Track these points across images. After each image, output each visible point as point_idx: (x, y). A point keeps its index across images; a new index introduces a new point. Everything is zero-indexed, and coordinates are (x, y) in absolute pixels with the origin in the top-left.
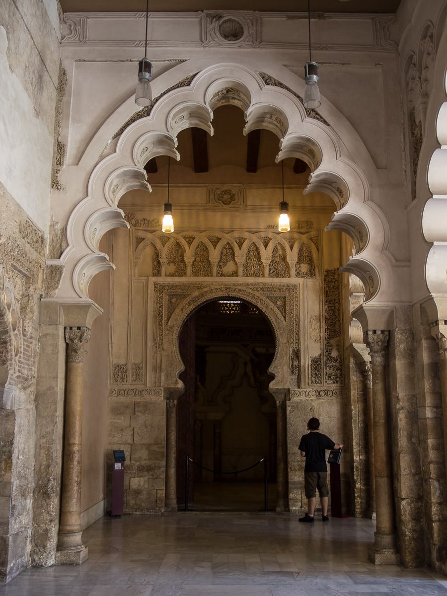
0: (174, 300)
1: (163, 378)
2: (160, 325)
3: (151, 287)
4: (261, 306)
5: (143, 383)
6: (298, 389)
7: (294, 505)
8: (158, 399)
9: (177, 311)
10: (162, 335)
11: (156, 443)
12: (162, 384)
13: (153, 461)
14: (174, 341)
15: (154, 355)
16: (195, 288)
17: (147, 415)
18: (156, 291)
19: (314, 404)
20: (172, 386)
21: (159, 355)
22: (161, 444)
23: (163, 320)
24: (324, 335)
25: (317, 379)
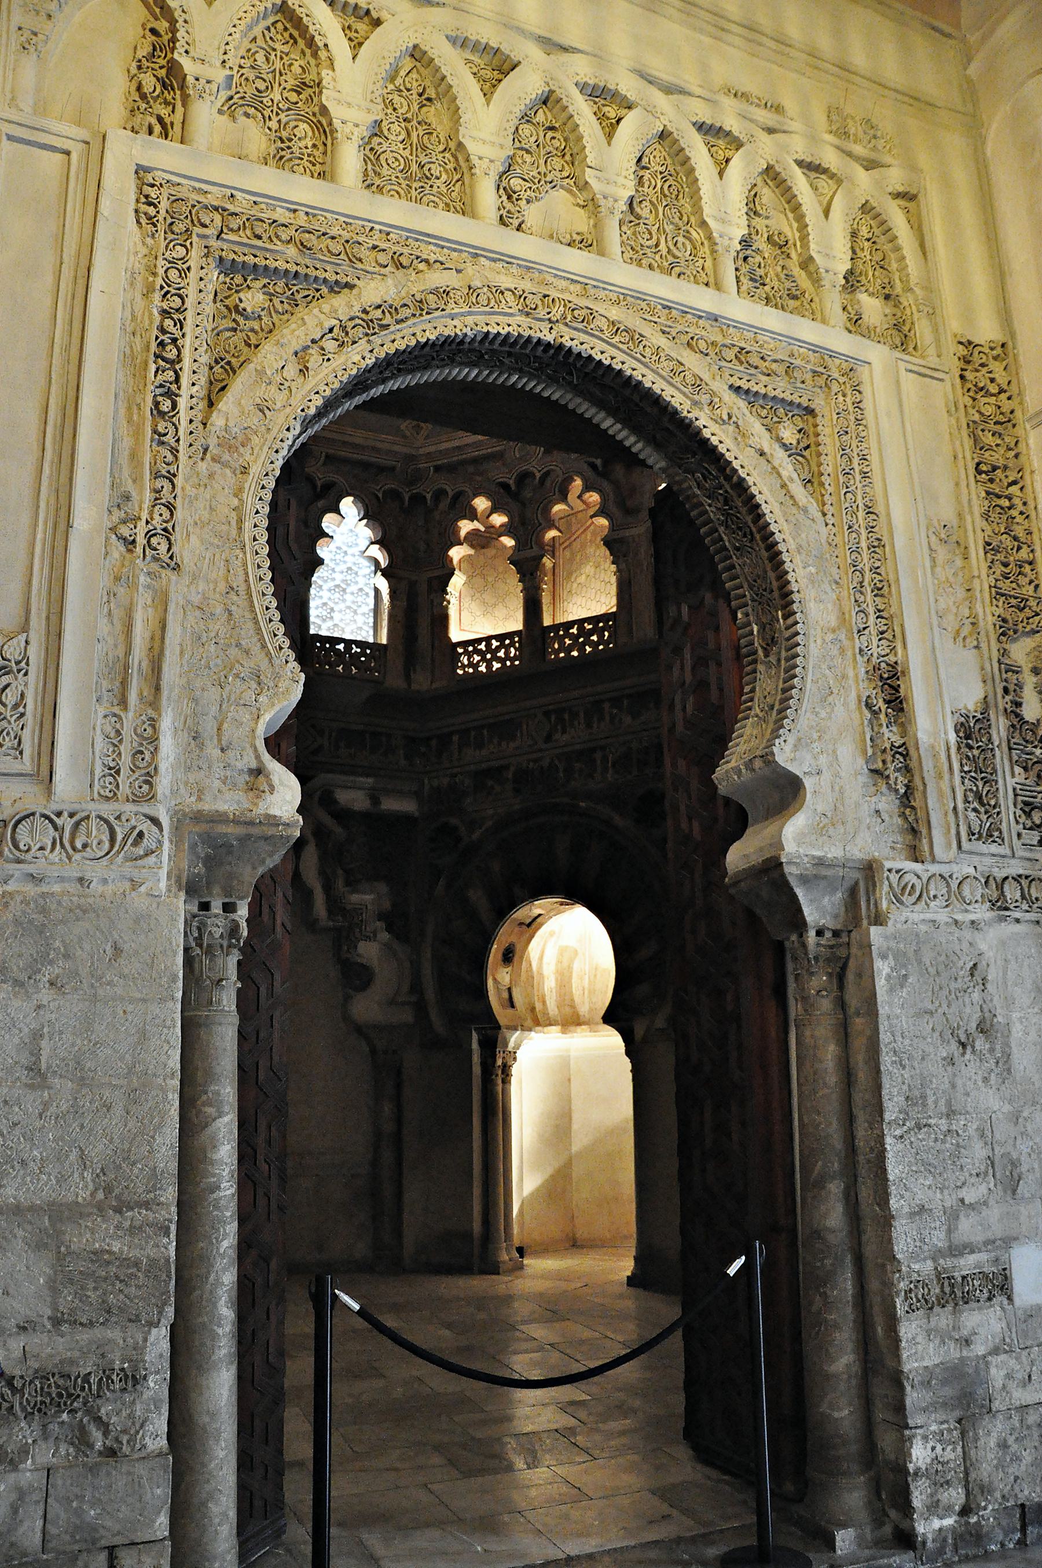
0: (253, 299)
1: (168, 745)
2: (164, 409)
3: (119, 193)
4: (713, 427)
5: (27, 764)
6: (917, 867)
7: (934, 1508)
8: (135, 885)
9: (270, 356)
10: (171, 477)
11: (115, 1200)
12: (163, 784)
13: (84, 1336)
14: (248, 525)
15: (111, 594)
16: (383, 258)
17: (45, 995)
18: (146, 219)
19: (983, 946)
20: (229, 802)
21: (143, 598)
22: (146, 1205)
23: (185, 390)
24: (988, 614)
25: (984, 817)
